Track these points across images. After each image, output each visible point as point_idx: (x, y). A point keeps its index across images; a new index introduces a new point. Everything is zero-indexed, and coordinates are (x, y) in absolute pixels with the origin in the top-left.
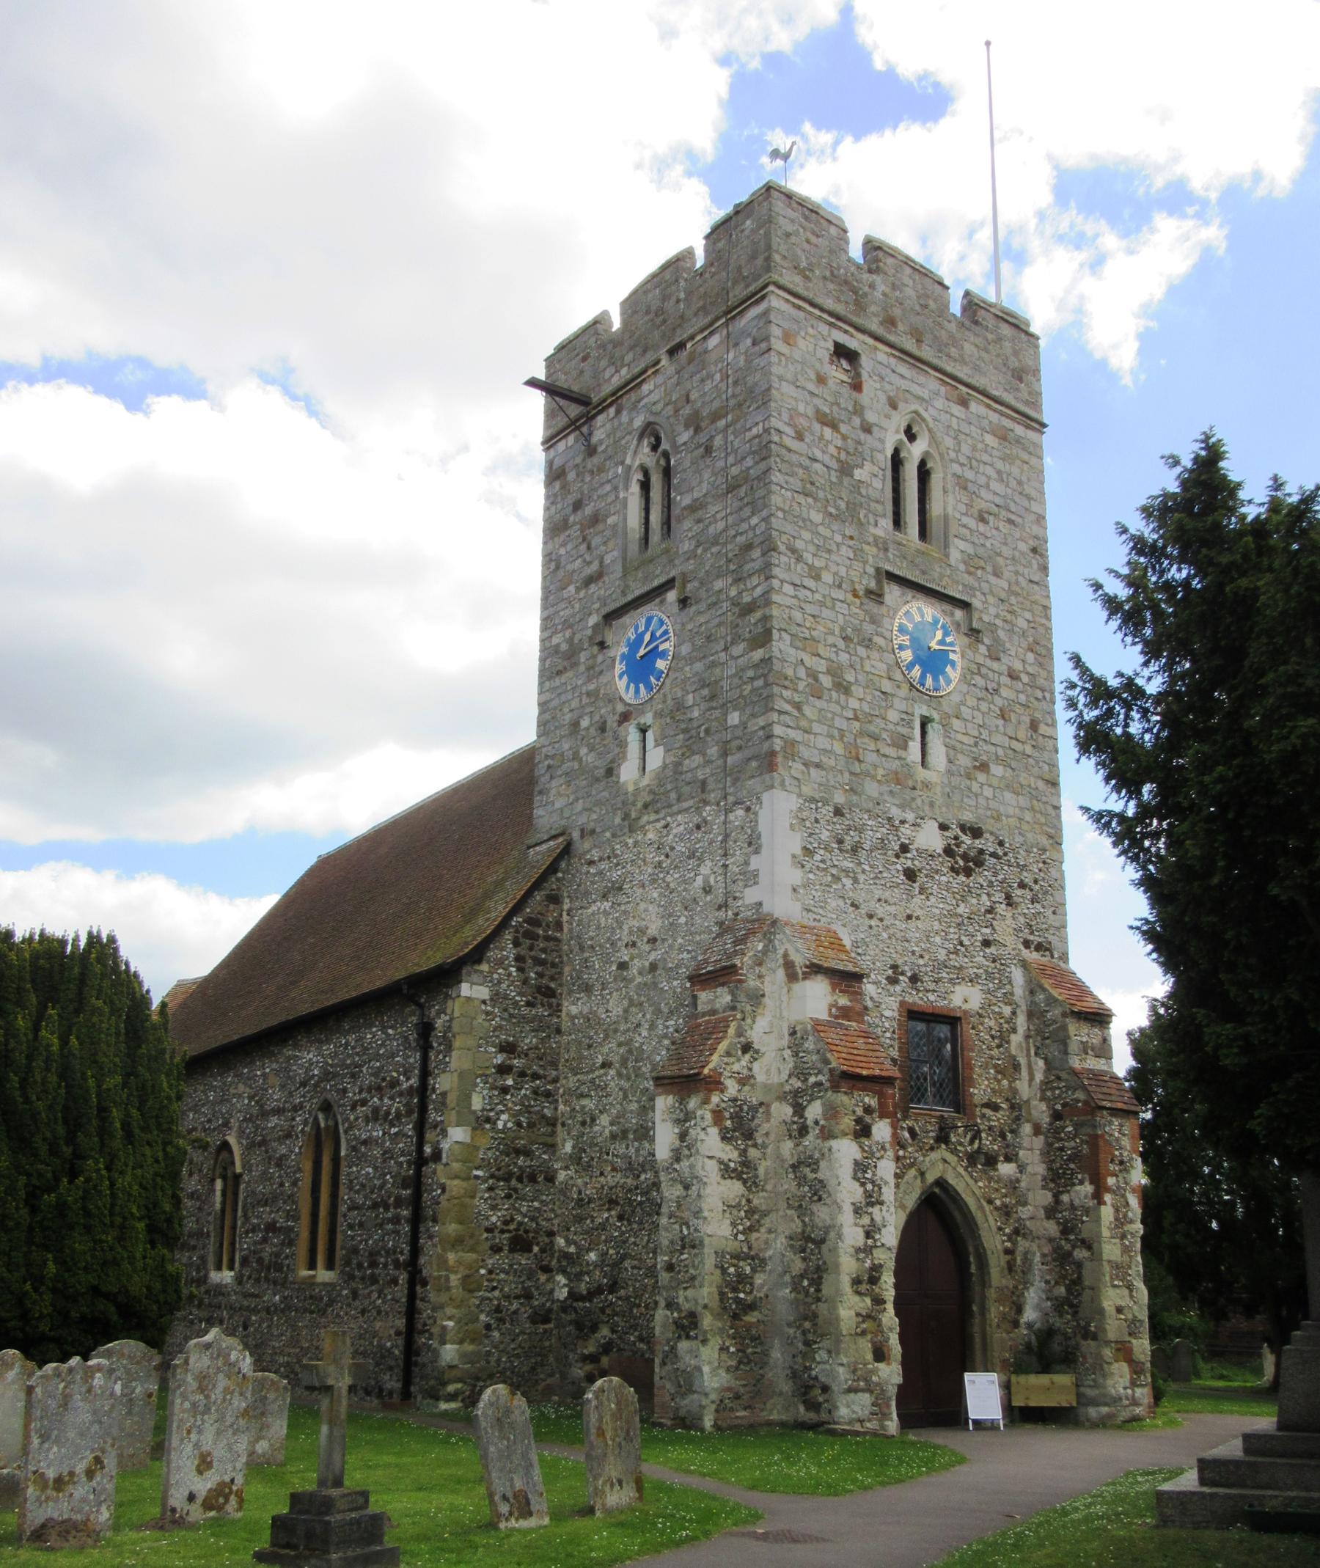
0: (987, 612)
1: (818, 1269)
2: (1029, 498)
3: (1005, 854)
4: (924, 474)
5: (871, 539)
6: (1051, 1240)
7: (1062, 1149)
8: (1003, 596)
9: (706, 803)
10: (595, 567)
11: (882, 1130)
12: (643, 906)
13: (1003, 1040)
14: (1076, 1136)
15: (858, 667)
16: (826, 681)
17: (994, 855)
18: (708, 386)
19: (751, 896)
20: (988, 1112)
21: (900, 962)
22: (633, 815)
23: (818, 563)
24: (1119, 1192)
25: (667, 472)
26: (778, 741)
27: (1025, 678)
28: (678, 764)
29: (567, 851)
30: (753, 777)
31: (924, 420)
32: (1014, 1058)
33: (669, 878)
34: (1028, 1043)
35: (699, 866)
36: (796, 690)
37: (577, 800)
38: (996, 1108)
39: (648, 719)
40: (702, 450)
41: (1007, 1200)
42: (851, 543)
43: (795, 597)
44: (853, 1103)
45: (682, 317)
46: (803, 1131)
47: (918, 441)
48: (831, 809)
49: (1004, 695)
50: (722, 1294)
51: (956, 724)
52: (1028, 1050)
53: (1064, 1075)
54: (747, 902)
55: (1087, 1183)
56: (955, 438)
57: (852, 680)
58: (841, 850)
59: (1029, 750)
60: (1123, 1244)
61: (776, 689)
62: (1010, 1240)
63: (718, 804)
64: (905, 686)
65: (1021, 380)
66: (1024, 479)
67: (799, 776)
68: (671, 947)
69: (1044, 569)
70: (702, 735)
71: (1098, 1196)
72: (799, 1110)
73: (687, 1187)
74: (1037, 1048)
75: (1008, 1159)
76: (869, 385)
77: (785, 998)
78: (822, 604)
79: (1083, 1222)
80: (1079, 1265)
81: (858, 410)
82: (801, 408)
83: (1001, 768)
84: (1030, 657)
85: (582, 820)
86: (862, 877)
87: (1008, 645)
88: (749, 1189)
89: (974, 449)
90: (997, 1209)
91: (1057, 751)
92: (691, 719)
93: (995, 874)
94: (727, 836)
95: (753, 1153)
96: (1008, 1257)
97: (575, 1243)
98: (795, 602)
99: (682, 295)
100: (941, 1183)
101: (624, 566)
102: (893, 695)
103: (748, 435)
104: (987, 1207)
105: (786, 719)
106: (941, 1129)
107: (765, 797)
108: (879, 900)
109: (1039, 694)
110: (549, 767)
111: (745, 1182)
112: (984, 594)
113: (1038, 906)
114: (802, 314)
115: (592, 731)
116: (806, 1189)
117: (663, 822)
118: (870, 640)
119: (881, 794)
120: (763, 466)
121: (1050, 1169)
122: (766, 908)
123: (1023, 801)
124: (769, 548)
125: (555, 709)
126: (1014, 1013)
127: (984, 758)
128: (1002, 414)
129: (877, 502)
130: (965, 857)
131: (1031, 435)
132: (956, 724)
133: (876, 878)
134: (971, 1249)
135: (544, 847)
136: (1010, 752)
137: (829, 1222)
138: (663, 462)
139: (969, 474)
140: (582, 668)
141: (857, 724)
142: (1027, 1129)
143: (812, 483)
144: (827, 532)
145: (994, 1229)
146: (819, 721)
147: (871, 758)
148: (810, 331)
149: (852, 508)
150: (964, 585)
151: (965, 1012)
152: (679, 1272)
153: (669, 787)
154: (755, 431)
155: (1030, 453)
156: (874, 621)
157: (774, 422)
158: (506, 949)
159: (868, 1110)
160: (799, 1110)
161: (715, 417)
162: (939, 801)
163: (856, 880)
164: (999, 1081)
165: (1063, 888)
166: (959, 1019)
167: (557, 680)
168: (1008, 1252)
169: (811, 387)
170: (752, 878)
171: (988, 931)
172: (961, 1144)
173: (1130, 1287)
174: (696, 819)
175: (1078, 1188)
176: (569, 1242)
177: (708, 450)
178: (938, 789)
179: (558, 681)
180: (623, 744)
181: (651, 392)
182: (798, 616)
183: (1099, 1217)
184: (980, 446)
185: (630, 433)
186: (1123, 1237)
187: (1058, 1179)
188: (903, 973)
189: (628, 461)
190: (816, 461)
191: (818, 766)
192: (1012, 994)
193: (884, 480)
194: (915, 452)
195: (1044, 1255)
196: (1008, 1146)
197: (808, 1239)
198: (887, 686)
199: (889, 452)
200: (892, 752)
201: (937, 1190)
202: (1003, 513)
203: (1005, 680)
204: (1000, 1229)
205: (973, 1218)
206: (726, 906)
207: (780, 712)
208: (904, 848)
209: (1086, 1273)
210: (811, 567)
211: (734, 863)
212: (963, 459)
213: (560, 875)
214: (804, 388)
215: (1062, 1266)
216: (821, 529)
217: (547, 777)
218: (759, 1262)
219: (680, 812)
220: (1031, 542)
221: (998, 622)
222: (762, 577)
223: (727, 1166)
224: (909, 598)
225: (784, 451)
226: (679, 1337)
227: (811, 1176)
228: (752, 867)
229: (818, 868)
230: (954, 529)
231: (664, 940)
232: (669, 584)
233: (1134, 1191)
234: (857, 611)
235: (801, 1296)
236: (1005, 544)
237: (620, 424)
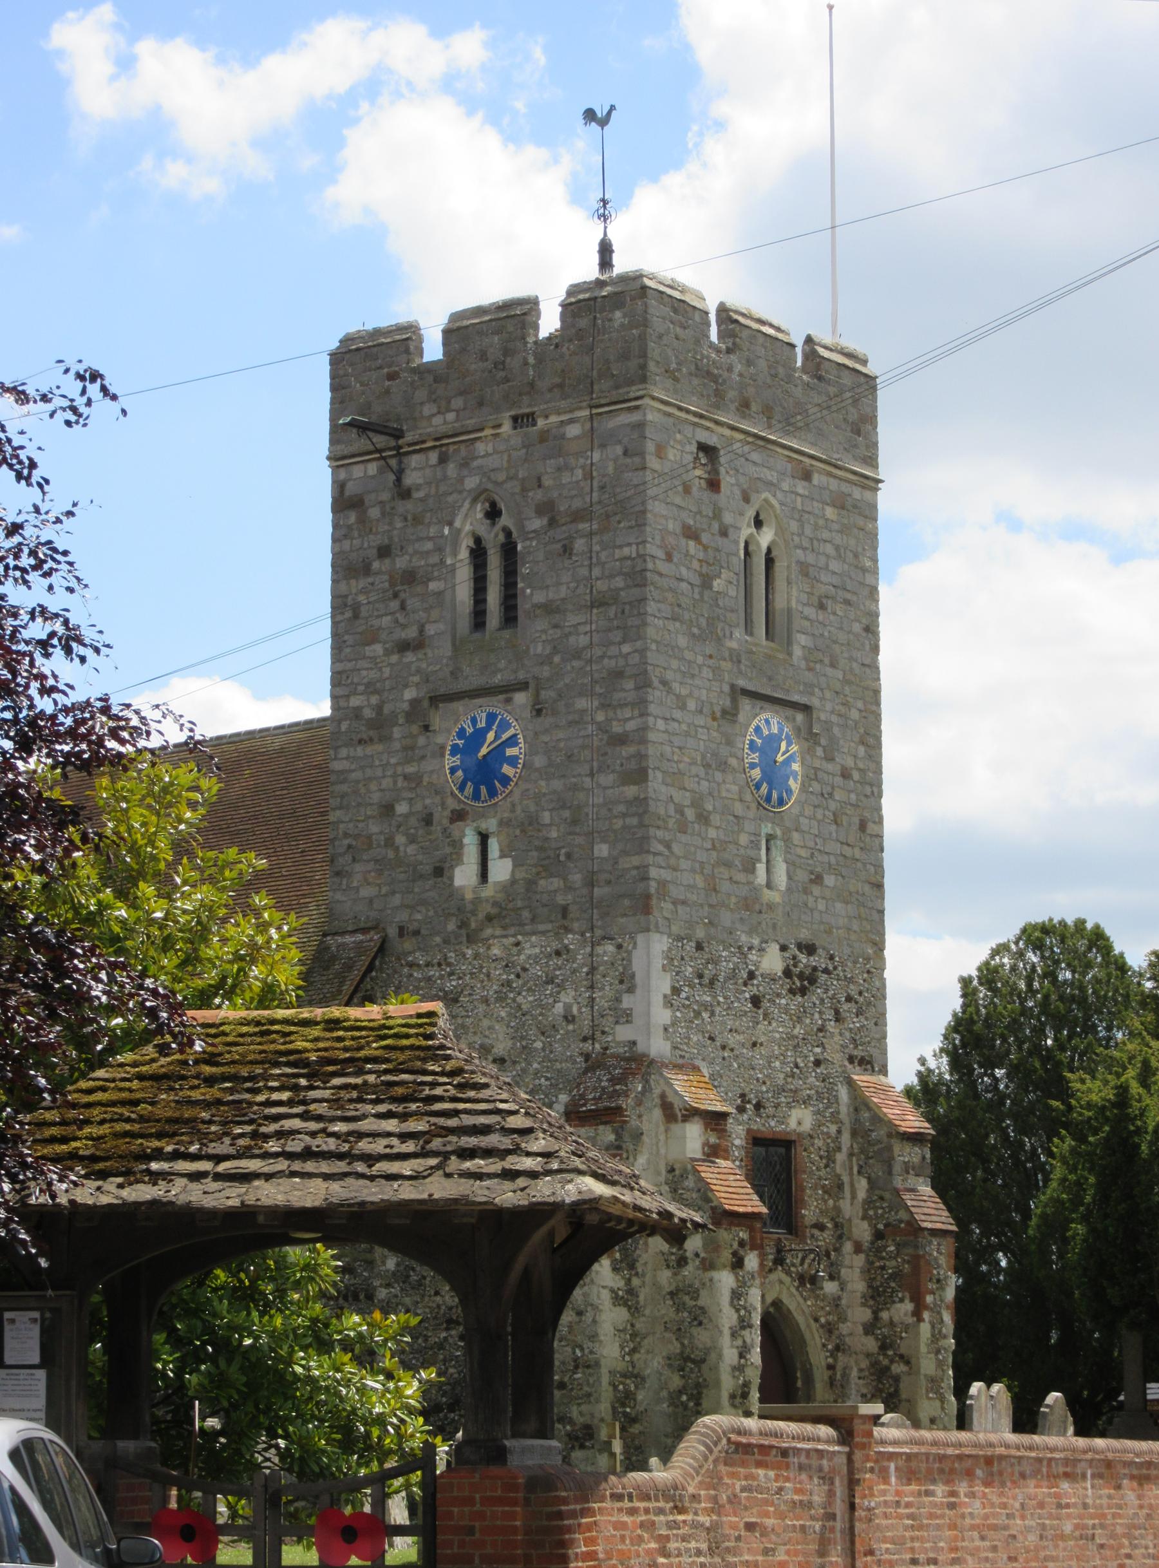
0: (825, 709)
1: (698, 1385)
2: (864, 570)
3: (835, 968)
4: (770, 561)
5: (727, 654)
6: (868, 1355)
7: (883, 1268)
8: (838, 686)
9: (567, 930)
10: (411, 633)
11: (752, 1261)
13: (830, 1160)
14: (898, 1254)
15: (716, 794)
16: (690, 814)
17: (826, 971)
18: (566, 478)
19: (623, 1033)
20: (816, 1232)
21: (747, 1090)
22: (473, 925)
23: (684, 692)
24: (936, 1310)
25: (509, 550)
26: (653, 884)
27: (856, 775)
28: (531, 884)
29: (382, 949)
30: (625, 915)
31: (772, 506)
32: (838, 1177)
33: (520, 999)
34: (851, 1161)
35: (559, 993)
36: (666, 828)
37: (393, 893)
38: (821, 1227)
39: (491, 824)
40: (559, 546)
41: (831, 1318)
42: (710, 662)
43: (666, 731)
44: (729, 1237)
45: (532, 385)
46: (682, 1261)
47: (765, 529)
48: (693, 944)
49: (837, 798)
50: (614, 1409)
51: (796, 836)
52: (851, 1169)
53: (887, 1195)
54: (619, 1038)
55: (907, 1301)
56: (799, 520)
57: (710, 808)
58: (700, 984)
59: (857, 853)
60: (937, 1359)
61: (652, 831)
62: (832, 1356)
63: (583, 934)
64: (754, 805)
65: (858, 433)
66: (860, 549)
67: (669, 916)
68: (524, 1070)
69: (876, 649)
70: (562, 858)
71: (917, 1314)
74: (861, 1167)
75: (832, 1278)
76: (727, 481)
77: (662, 1137)
78: (687, 734)
79: (901, 1338)
80: (897, 1379)
81: (717, 514)
82: (671, 526)
83: (833, 877)
84: (862, 750)
85: (403, 916)
86: (718, 1010)
87: (841, 742)
88: (632, 1315)
89: (816, 527)
90: (822, 1326)
91: (882, 850)
92: (547, 839)
93: (826, 991)
94: (593, 970)
95: (636, 1282)
96: (830, 1372)
98: (665, 736)
99: (531, 360)
100: (777, 1304)
101: (454, 644)
102: (743, 818)
103: (618, 554)
104: (814, 1325)
105: (659, 859)
106: (779, 1251)
107: (640, 938)
108: (731, 1030)
109: (868, 790)
110: (350, 846)
111: (629, 1308)
112: (822, 690)
113: (862, 1018)
114: (671, 420)
115: (413, 821)
116: (686, 1314)
117: (512, 940)
118: (726, 763)
119: (733, 923)
120: (636, 592)
121: (870, 1287)
122: (641, 1048)
124: (643, 683)
125: (358, 782)
126: (839, 1132)
127: (819, 869)
129: (732, 611)
130: (801, 976)
131: (868, 494)
132: (796, 836)
133: (729, 1008)
134: (798, 1365)
135: (348, 939)
136: (841, 859)
137: (709, 1344)
138: (501, 538)
139: (811, 559)
140: (397, 745)
141: (714, 854)
142: (848, 1247)
143: (679, 606)
145: (819, 1345)
146: (686, 858)
147: (725, 887)
148: (678, 436)
149: (711, 622)
150: (805, 684)
151: (799, 1134)
152: (572, 1389)
153: (520, 904)
154: (626, 551)
155: (866, 517)
156: (729, 743)
157: (651, 549)
159: (742, 1244)
161: (577, 516)
163: (713, 1014)
164: (825, 1202)
165: (884, 997)
166: (795, 1141)
167: (359, 749)
168: (830, 1367)
169: (678, 500)
170: (626, 1017)
171: (818, 1050)
172: (793, 1265)
173: (942, 1399)
174: (556, 945)
175: (898, 1305)
177: (567, 550)
178: (780, 909)
179: (360, 751)
180: (457, 846)
181: (487, 455)
182: (668, 749)
183: (918, 1334)
184: (821, 522)
185: (460, 492)
186: (938, 1352)
187: (878, 1296)
188: (749, 1102)
189: (457, 524)
190: (682, 580)
191: (684, 903)
192: (838, 1113)
193: (738, 586)
194: (765, 538)
195: (861, 1370)
196: (832, 1264)
197: (687, 1359)
198: (738, 809)
199: (742, 545)
200: (741, 877)
201: (771, 1310)
202: (840, 593)
203: (839, 780)
204: (824, 1345)
205: (802, 1336)
206: (593, 1039)
207: (655, 854)
208: (751, 975)
209: (902, 1385)
210: (678, 696)
211: (602, 997)
212: (806, 544)
213: (374, 974)
214: (673, 504)
215: (879, 1380)
216: (688, 655)
217: (348, 857)
218: (639, 1378)
219: (534, 933)
220: (864, 621)
221: (834, 719)
222: (636, 712)
223: (617, 1294)
224: (758, 711)
225: (657, 578)
226: (573, 1448)
227: (691, 1303)
228: (625, 1005)
229: (683, 1006)
230: (798, 623)
231: (514, 1063)
233: (948, 1308)
234: (715, 734)
235: (681, 1409)
236: (841, 628)
237: (445, 477)
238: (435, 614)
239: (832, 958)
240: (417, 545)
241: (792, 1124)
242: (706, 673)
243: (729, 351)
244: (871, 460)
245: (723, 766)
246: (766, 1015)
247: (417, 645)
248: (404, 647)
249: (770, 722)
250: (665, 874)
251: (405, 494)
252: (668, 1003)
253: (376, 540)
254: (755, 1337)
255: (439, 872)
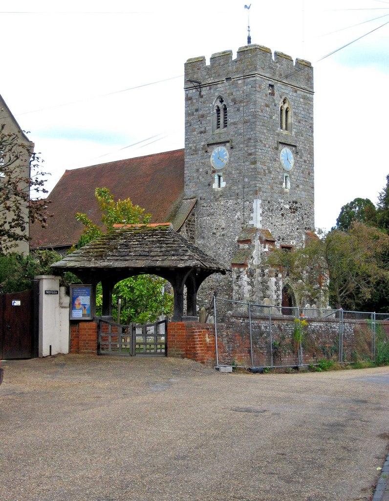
0: (300, 146)
2: (310, 114)
4: (287, 112)
10: (203, 129)
11: (280, 275)
12: (220, 220)
16: (267, 171)
17: (300, 208)
19: (251, 222)
25: (225, 109)
27: (308, 162)
28: (230, 188)
29: (196, 202)
39: (221, 174)
46: (264, 275)
51: (293, 176)
69: (312, 132)
72: (263, 271)
73: (240, 287)
76: (276, 93)
81: (274, 101)
84: (309, 156)
85: (201, 195)
86: (273, 217)
95: (253, 280)
97: (201, 298)
107: (255, 200)
115: (204, 173)
122: (255, 226)
123: (306, 194)
125: (191, 164)
128: (304, 92)
130: (294, 209)
131: (311, 96)
132: (293, 176)
140: (200, 155)
142: (305, 272)
144: (266, 134)
147: (275, 188)
154: (252, 110)
158: (184, 229)
160: (263, 271)
162: (288, 196)
163: (272, 218)
167: (191, 156)
169: (264, 98)
170: (252, 219)
174: (235, 202)
176: (199, 298)
177: (238, 110)
180: (213, 179)
189: (213, 104)
191: (265, 192)
194: (286, 106)
198: (279, 170)
200: (279, 186)
203: (303, 163)
208: (281, 209)
230: (293, 126)
232: (228, 142)
238: (208, 125)
239: (301, 205)
240: (204, 109)
241: (291, 243)
242: (271, 138)
243: (277, 63)
244: (312, 88)
245: (275, 160)
246: (285, 218)
247: (204, 132)
248: (201, 132)
249: (285, 151)
250: (261, 185)
251: (202, 97)
252: (261, 215)
253: (195, 107)
254: (280, 292)
255: (209, 185)
